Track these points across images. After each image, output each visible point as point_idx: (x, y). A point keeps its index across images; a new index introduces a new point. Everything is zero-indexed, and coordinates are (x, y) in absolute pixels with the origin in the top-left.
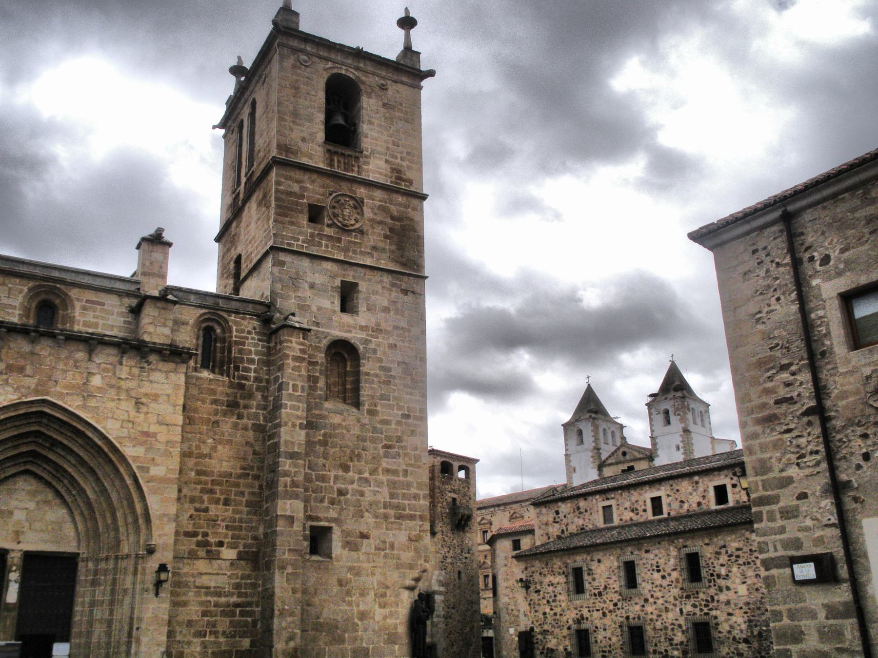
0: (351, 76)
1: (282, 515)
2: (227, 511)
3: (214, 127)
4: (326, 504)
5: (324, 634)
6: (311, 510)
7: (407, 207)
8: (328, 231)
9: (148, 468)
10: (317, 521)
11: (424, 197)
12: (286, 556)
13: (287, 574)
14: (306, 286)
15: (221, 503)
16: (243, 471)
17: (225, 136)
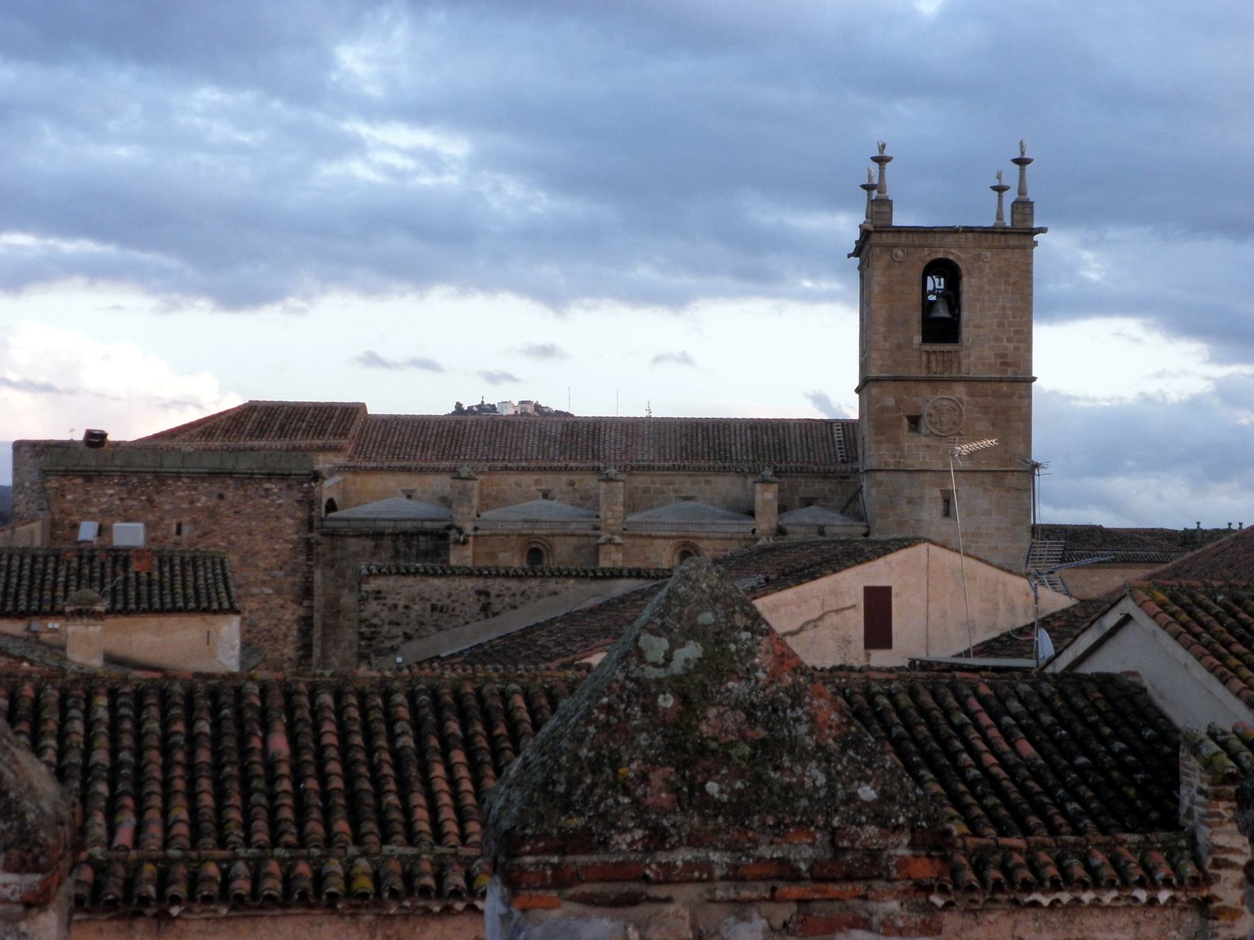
0: (951, 257)
3: (849, 256)
7: (1011, 396)
8: (924, 440)
11: (1034, 379)
14: (904, 501)
17: (860, 268)
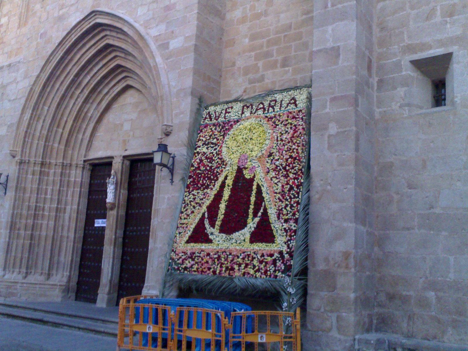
1: (320, 51)
2: (287, 72)
4: (438, 19)
5: (444, 233)
6: (409, 37)
9: (168, 43)
10: (422, 50)
12: (327, 110)
13: (330, 136)
15: (279, 65)
16: (304, 17)
